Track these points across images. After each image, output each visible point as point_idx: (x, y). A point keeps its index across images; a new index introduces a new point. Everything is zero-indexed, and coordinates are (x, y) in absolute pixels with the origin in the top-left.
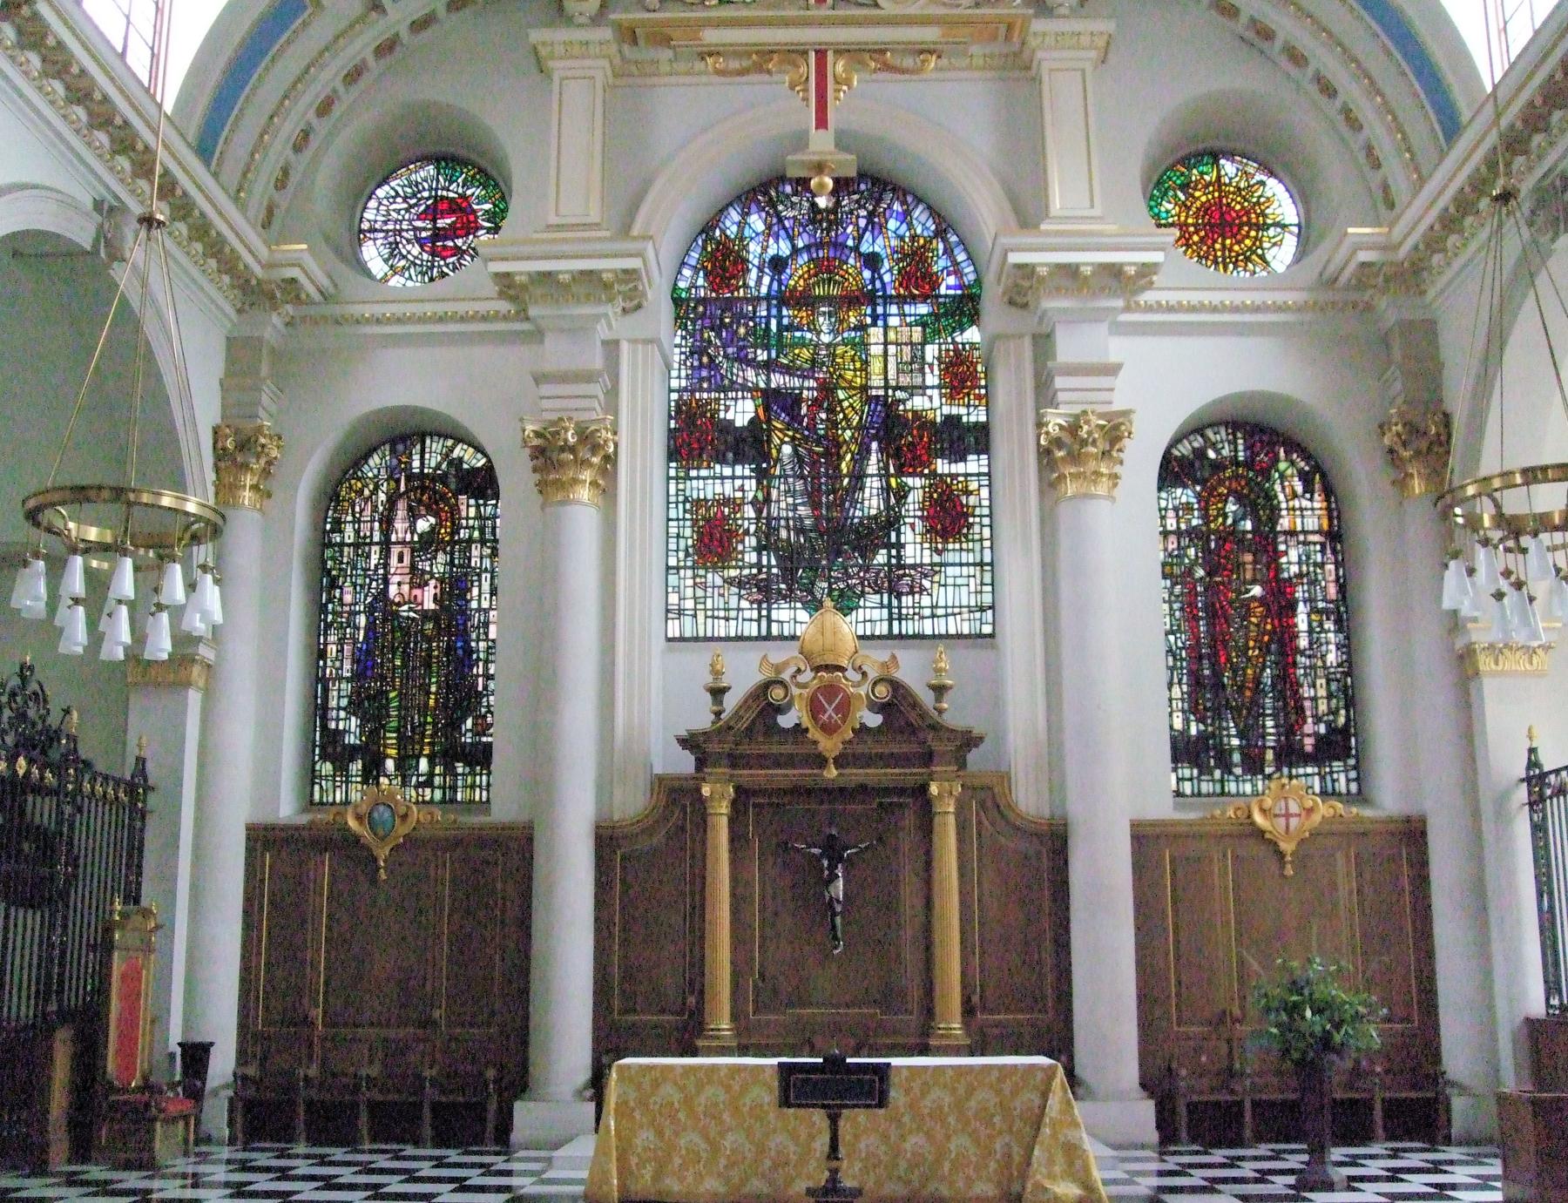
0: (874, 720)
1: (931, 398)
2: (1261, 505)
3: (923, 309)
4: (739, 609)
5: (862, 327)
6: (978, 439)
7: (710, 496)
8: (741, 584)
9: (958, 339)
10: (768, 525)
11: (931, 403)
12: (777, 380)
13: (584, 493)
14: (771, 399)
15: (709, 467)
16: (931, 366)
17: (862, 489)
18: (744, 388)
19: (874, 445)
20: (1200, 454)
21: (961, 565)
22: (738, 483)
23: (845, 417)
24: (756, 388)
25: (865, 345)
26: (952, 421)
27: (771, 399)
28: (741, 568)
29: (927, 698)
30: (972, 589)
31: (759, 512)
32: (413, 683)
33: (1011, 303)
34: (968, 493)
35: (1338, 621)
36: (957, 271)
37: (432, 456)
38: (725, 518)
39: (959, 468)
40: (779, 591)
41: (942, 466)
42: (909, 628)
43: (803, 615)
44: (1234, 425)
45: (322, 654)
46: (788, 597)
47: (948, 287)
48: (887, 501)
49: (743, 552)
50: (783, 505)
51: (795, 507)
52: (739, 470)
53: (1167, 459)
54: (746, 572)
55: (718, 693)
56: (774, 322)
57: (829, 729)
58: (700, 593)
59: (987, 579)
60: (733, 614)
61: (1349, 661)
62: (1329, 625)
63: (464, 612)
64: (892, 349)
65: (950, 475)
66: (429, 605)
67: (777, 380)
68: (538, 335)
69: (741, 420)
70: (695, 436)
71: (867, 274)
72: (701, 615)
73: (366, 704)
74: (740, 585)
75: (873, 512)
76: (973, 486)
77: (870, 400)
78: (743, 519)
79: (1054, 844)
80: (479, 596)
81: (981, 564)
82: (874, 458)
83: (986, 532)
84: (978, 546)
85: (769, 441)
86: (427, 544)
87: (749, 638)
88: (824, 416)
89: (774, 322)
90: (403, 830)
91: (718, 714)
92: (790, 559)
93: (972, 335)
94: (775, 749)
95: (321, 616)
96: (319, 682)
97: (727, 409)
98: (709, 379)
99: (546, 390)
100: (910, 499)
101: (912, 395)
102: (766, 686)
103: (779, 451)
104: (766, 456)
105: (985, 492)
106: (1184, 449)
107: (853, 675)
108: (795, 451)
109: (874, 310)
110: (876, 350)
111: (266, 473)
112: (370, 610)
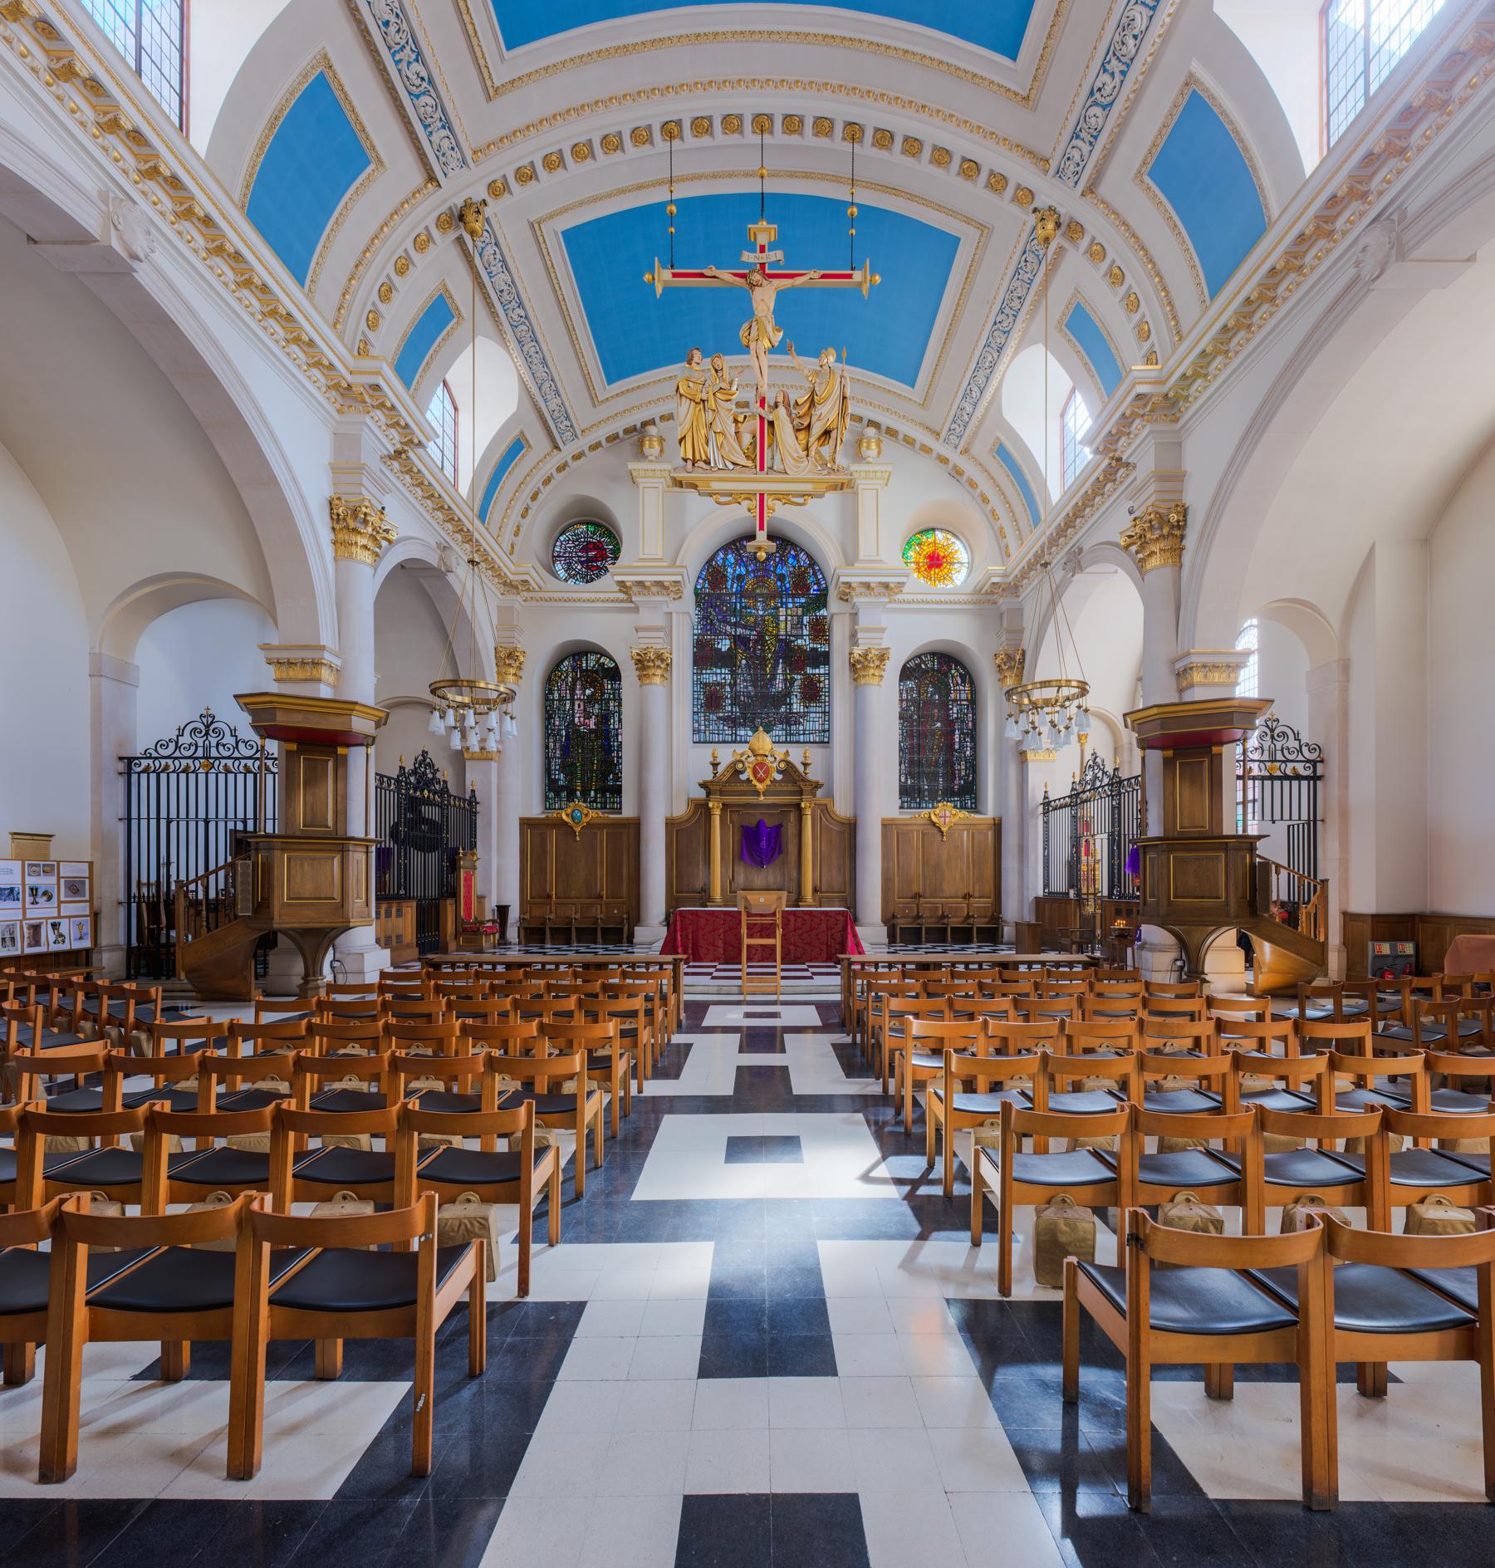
0: (779, 777)
2: (943, 688)
3: (803, 600)
5: (777, 608)
8: (724, 719)
11: (805, 642)
12: (739, 631)
13: (658, 680)
14: (738, 640)
20: (918, 666)
25: (776, 617)
26: (814, 650)
27: (738, 640)
29: (801, 768)
32: (585, 757)
36: (818, 583)
37: (591, 662)
41: (809, 670)
42: (794, 738)
44: (933, 654)
45: (547, 747)
46: (744, 725)
53: (904, 667)
55: (715, 765)
63: (608, 731)
66: (593, 726)
67: (739, 631)
68: (636, 610)
69: (724, 649)
70: (704, 656)
73: (564, 768)
74: (724, 719)
77: (780, 641)
79: (851, 829)
80: (613, 723)
86: (590, 700)
90: (585, 820)
92: (744, 707)
93: (823, 612)
95: (549, 731)
96: (548, 760)
99: (641, 634)
102: (735, 763)
106: (912, 664)
107: (771, 759)
111: (519, 668)
112: (567, 728)
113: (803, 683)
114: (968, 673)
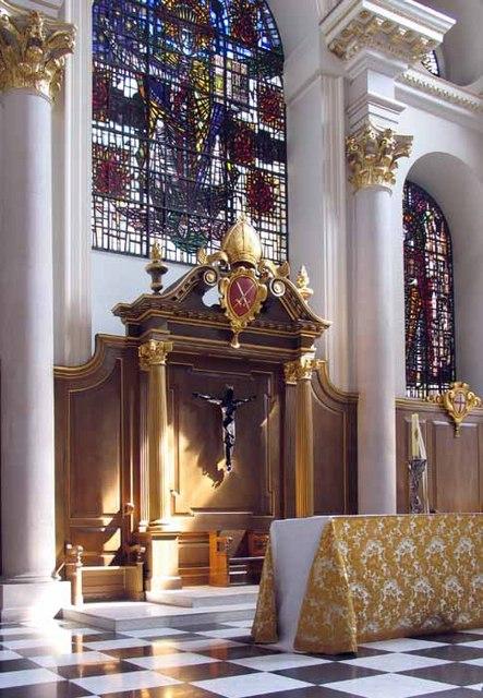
1: (252, 115)
4: (127, 232)
5: (212, 54)
6: (279, 152)
7: (106, 143)
9: (269, 81)
10: (147, 175)
12: (153, 71)
14: (147, 81)
15: (104, 121)
16: (253, 94)
17: (210, 165)
18: (130, 68)
19: (218, 138)
21: (269, 231)
22: (126, 139)
23: (199, 112)
24: (137, 72)
25: (211, 66)
28: (129, 202)
30: (275, 249)
31: (141, 164)
33: (334, 52)
34: (274, 186)
35: (449, 307)
38: (116, 163)
39: (269, 167)
40: (155, 225)
41: (258, 163)
43: (171, 246)
46: (162, 230)
47: (263, 44)
48: (225, 178)
49: (129, 191)
50: (158, 163)
51: (165, 167)
52: (127, 129)
54: (132, 206)
56: (151, 27)
57: (240, 311)
58: (98, 214)
59: (284, 245)
60: (123, 235)
61: (453, 328)
62: (445, 308)
64: (229, 74)
65: (263, 170)
71: (213, 15)
72: (99, 231)
74: (128, 215)
75: (217, 183)
76: (276, 182)
78: (130, 167)
81: (280, 234)
82: (217, 147)
83: (284, 213)
84: (278, 223)
85: (149, 114)
87: (134, 255)
88: (185, 107)
89: (151, 27)
91: (157, 289)
93: (275, 80)
94: (199, 323)
97: (118, 82)
98: (105, 54)
100: (239, 181)
101: (241, 110)
103: (155, 124)
104: (147, 126)
105: (283, 188)
108: (166, 129)
109: (218, 43)
110: (219, 71)
113: (250, 182)
114: (443, 219)
